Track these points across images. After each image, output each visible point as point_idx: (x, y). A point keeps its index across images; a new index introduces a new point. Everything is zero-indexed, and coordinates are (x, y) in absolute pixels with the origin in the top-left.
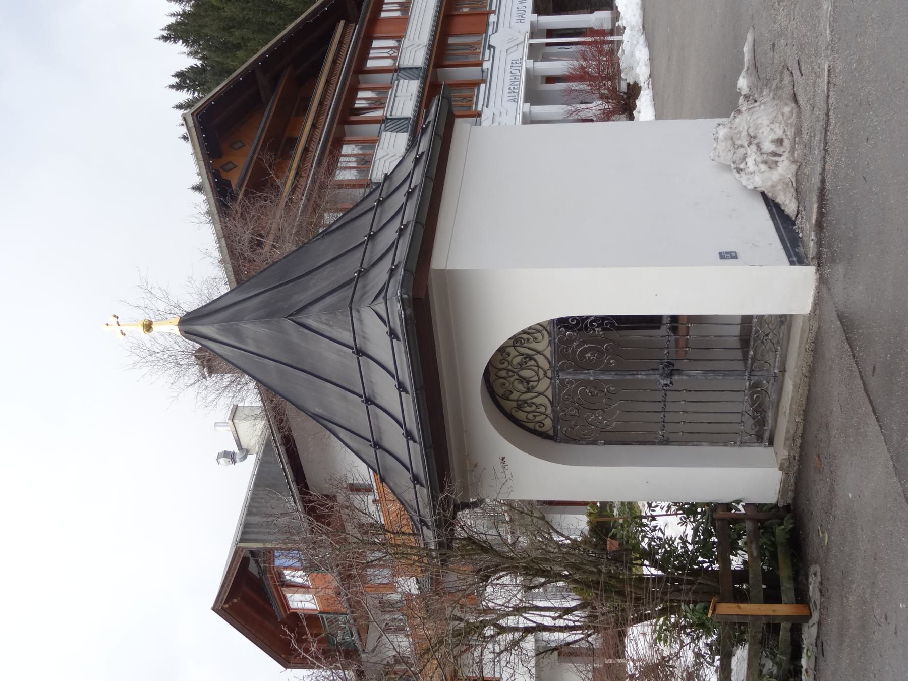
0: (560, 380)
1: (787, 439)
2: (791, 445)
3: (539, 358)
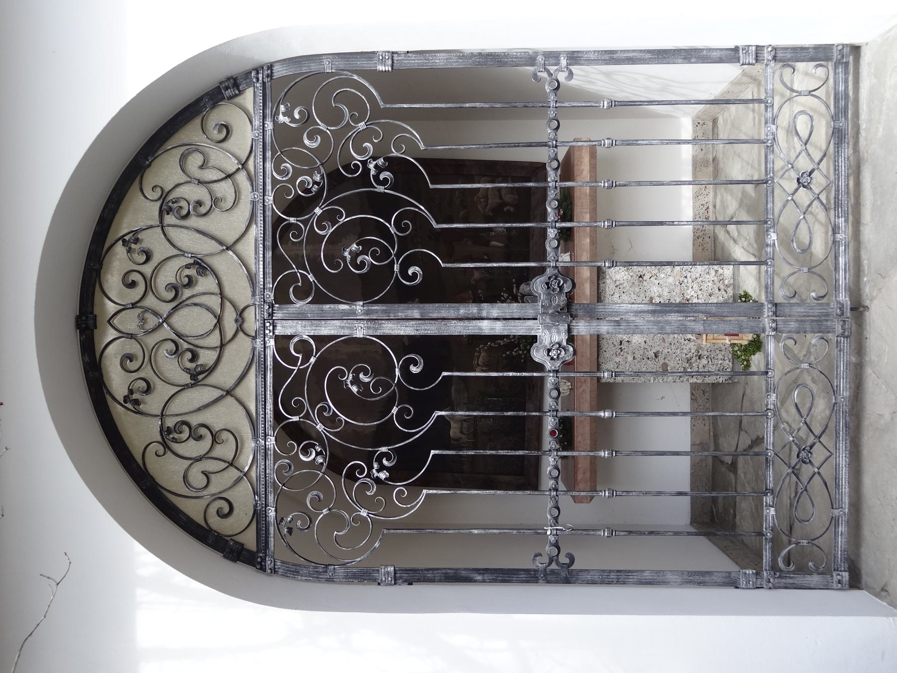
0: (277, 338)
3: (225, 264)
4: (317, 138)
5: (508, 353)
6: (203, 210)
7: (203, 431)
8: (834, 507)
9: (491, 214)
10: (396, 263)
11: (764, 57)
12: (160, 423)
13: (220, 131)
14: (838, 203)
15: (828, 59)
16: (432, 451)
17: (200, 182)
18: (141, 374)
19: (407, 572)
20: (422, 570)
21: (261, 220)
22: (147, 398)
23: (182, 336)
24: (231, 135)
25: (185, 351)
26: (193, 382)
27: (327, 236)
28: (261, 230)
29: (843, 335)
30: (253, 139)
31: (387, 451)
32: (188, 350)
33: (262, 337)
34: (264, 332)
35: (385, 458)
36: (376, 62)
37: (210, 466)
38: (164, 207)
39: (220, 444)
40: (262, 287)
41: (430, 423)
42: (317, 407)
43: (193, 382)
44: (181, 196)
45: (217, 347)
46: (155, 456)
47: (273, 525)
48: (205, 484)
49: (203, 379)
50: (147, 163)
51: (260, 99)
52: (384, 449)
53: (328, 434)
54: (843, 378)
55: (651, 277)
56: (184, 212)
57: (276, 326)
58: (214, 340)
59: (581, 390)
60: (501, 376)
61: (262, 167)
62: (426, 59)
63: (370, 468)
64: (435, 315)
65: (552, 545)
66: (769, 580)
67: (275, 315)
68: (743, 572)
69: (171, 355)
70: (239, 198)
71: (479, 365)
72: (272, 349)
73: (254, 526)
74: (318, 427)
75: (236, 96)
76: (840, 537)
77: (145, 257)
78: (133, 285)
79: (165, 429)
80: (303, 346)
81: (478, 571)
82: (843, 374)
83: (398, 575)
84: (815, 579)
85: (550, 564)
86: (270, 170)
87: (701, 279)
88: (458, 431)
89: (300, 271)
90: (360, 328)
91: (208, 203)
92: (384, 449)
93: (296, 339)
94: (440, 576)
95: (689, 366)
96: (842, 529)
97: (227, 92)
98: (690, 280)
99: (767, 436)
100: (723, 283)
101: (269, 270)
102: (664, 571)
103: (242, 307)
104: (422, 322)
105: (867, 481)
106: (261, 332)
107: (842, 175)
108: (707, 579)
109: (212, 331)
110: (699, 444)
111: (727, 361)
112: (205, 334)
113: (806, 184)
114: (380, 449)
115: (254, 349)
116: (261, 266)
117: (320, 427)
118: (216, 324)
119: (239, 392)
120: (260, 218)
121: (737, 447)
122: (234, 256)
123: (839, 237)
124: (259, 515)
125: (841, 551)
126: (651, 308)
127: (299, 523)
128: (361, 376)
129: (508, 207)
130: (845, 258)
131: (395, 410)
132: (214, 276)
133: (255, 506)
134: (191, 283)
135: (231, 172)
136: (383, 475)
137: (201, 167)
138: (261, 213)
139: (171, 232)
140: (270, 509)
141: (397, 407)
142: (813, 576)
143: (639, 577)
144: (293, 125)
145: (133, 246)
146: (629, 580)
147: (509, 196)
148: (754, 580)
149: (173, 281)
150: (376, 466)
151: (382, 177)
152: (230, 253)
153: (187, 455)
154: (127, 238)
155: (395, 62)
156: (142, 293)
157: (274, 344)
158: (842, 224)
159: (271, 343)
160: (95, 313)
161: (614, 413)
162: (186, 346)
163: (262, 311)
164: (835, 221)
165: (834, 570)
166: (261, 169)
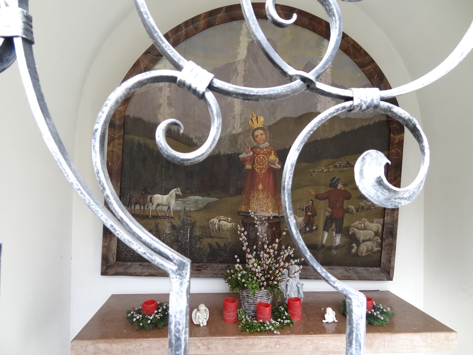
9: (350, 233)
41: (134, 234)
59: (200, 345)
71: (219, 221)
88: (159, 201)
129: (356, 247)
147: (365, 248)
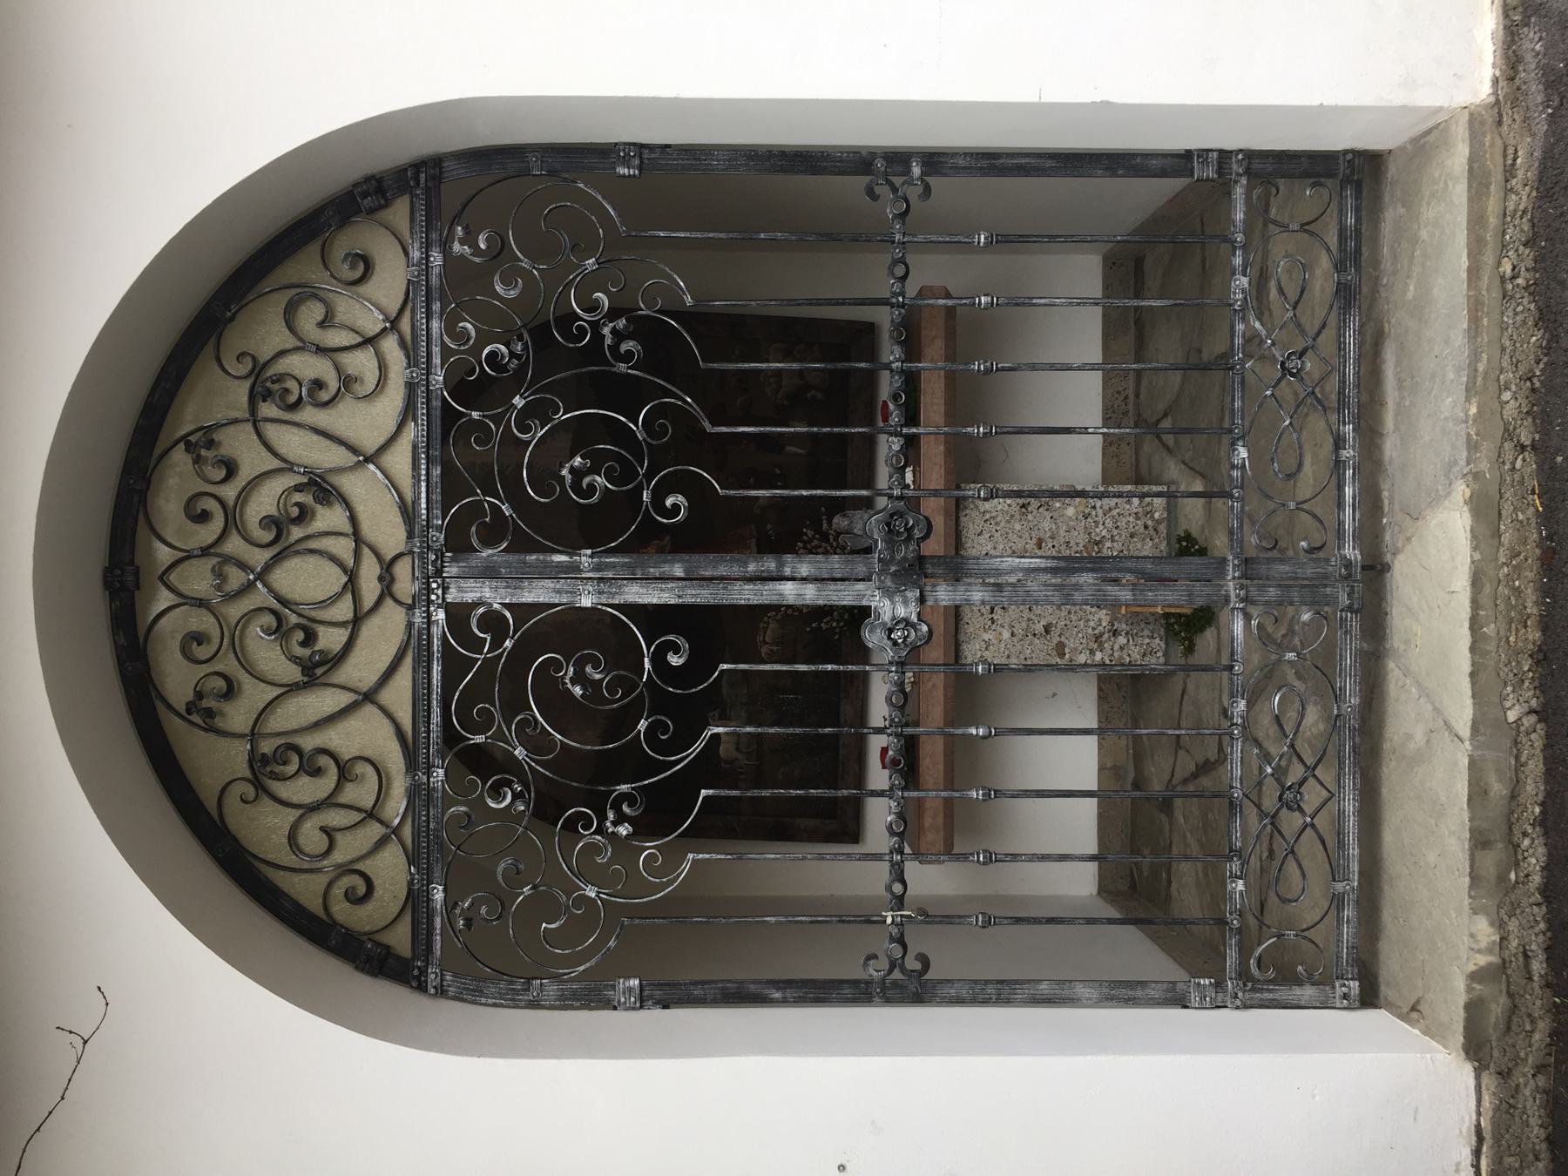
0: (450, 609)
1: (1479, 842)
2: (1502, 878)
3: (364, 489)
4: (517, 281)
5: (814, 625)
6: (324, 396)
7: (324, 761)
8: (1337, 879)
10: (645, 487)
11: (1231, 169)
12: (249, 747)
13: (353, 267)
14: (1344, 401)
15: (1331, 174)
16: (703, 791)
17: (321, 350)
18: (218, 666)
19: (660, 988)
20: (685, 984)
21: (423, 414)
22: (228, 708)
23: (289, 602)
24: (372, 272)
25: (293, 628)
26: (306, 679)
27: (533, 443)
28: (423, 430)
29: (1350, 608)
30: (409, 280)
31: (630, 791)
32: (298, 626)
33: (424, 606)
34: (429, 598)
35: (626, 803)
36: (614, 160)
37: (335, 818)
38: (259, 389)
39: (352, 781)
40: (425, 523)
42: (516, 721)
43: (306, 679)
44: (289, 371)
45: (347, 622)
46: (239, 799)
47: (440, 915)
48: (326, 848)
49: (325, 673)
50: (229, 314)
51: (422, 215)
52: (624, 788)
53: (533, 764)
54: (1350, 675)
55: (1039, 508)
56: (293, 399)
57: (448, 588)
58: (344, 610)
60: (813, 671)
61: (424, 327)
62: (695, 159)
63: (602, 818)
64: (708, 574)
65: (892, 939)
66: (1236, 994)
67: (446, 569)
68: (1195, 982)
69: (270, 635)
70: (386, 376)
71: (765, 643)
72: (441, 625)
73: (408, 918)
74: (516, 752)
75: (381, 207)
76: (1345, 926)
77: (223, 473)
78: (203, 517)
79: (258, 757)
80: (493, 622)
81: (776, 984)
82: (1350, 670)
83: (646, 993)
84: (1308, 992)
85: (890, 971)
86: (438, 330)
87: (1117, 510)
89: (487, 498)
90: (586, 592)
91: (333, 384)
92: (624, 788)
93: (481, 610)
94: (715, 994)
95: (1099, 646)
96: (1349, 912)
97: (366, 201)
98: (1100, 512)
99: (1232, 767)
100: (1152, 517)
101: (436, 497)
102: (1071, 981)
103: (389, 557)
104: (688, 583)
105: (1388, 837)
106: (424, 597)
107: (1350, 358)
108: (1139, 993)
109: (338, 596)
110: (1110, 769)
111: (1157, 640)
112: (328, 600)
113: (1295, 371)
114: (618, 788)
115: (410, 625)
116: (423, 489)
117: (519, 752)
118: (346, 584)
119: (387, 696)
120: (422, 411)
121: (1173, 775)
122: (378, 472)
123: (1347, 453)
124: (416, 900)
125: (1347, 948)
126: (1050, 563)
127: (483, 910)
128: (588, 669)
129: (813, 392)
130: (1354, 487)
131: (642, 725)
132: (344, 505)
133: (411, 883)
134: (304, 515)
135: (372, 334)
136: (623, 830)
137: (322, 325)
138: (423, 403)
139: (271, 431)
140: (435, 888)
141: (646, 720)
142: (1304, 987)
143: (1032, 992)
144: (477, 260)
145: (203, 452)
146: (1016, 996)
148: (1213, 995)
149: (273, 511)
150: (611, 816)
151: (624, 347)
152: (371, 467)
153: (295, 799)
154: (193, 439)
155: (645, 161)
156: (219, 531)
157: (444, 617)
158: (1349, 434)
159: (441, 615)
160: (137, 562)
161: (993, 731)
162: (294, 619)
163: (424, 563)
164: (1339, 430)
165: (1337, 978)
166: (423, 330)
